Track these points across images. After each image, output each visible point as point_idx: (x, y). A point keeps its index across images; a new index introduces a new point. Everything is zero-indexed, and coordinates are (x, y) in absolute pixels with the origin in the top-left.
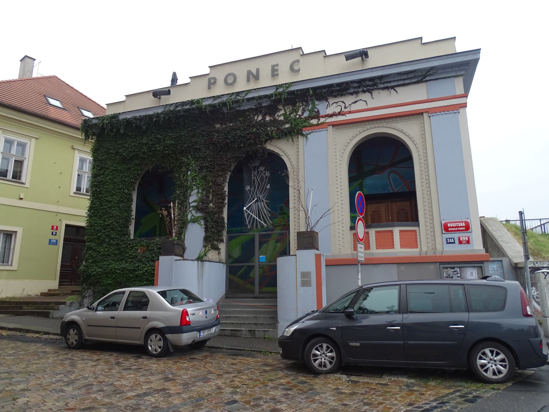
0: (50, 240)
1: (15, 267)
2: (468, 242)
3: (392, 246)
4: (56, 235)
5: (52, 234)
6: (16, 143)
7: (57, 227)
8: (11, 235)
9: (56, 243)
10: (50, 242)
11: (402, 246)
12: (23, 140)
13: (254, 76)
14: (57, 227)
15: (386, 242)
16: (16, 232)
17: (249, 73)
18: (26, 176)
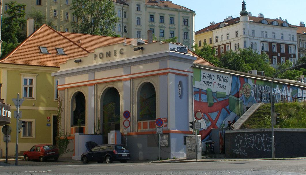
0: (47, 124)
1: (34, 137)
2: (166, 126)
3: (147, 128)
4: (49, 121)
5: (48, 121)
6: (28, 80)
7: (50, 117)
8: (31, 123)
9: (50, 125)
10: (47, 125)
11: (150, 128)
12: (31, 78)
13: (108, 55)
14: (50, 117)
15: (145, 127)
16: (33, 121)
17: (107, 53)
18: (34, 95)
